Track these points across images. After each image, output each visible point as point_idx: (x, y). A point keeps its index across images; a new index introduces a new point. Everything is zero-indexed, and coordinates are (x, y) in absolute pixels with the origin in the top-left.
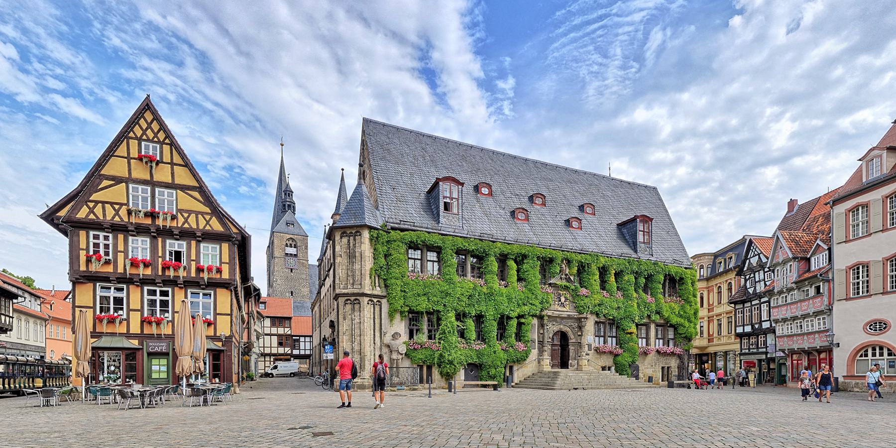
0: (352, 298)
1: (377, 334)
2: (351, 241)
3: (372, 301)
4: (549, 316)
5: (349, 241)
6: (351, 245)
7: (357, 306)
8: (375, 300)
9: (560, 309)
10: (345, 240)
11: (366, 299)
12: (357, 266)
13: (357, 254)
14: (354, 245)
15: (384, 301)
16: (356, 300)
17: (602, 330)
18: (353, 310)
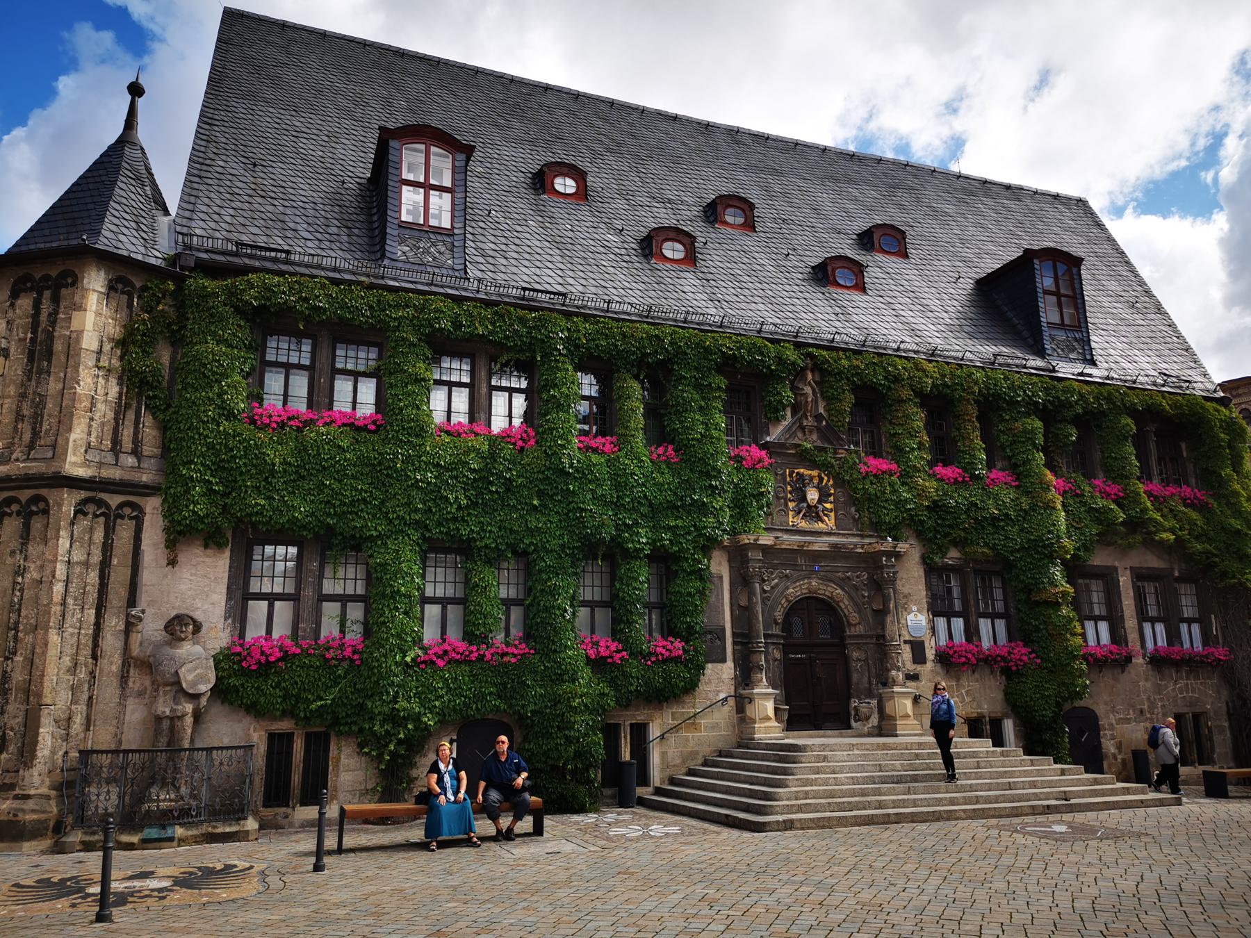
0: (24, 495)
1: (113, 623)
2: (46, 307)
3: (100, 503)
4: (765, 549)
5: (37, 305)
6: (44, 317)
7: (37, 524)
8: (114, 500)
9: (804, 525)
10: (25, 303)
11: (68, 502)
12: (53, 386)
13: (58, 346)
14: (53, 321)
15: (152, 506)
16: (37, 499)
17: (956, 592)
18: (25, 536)
